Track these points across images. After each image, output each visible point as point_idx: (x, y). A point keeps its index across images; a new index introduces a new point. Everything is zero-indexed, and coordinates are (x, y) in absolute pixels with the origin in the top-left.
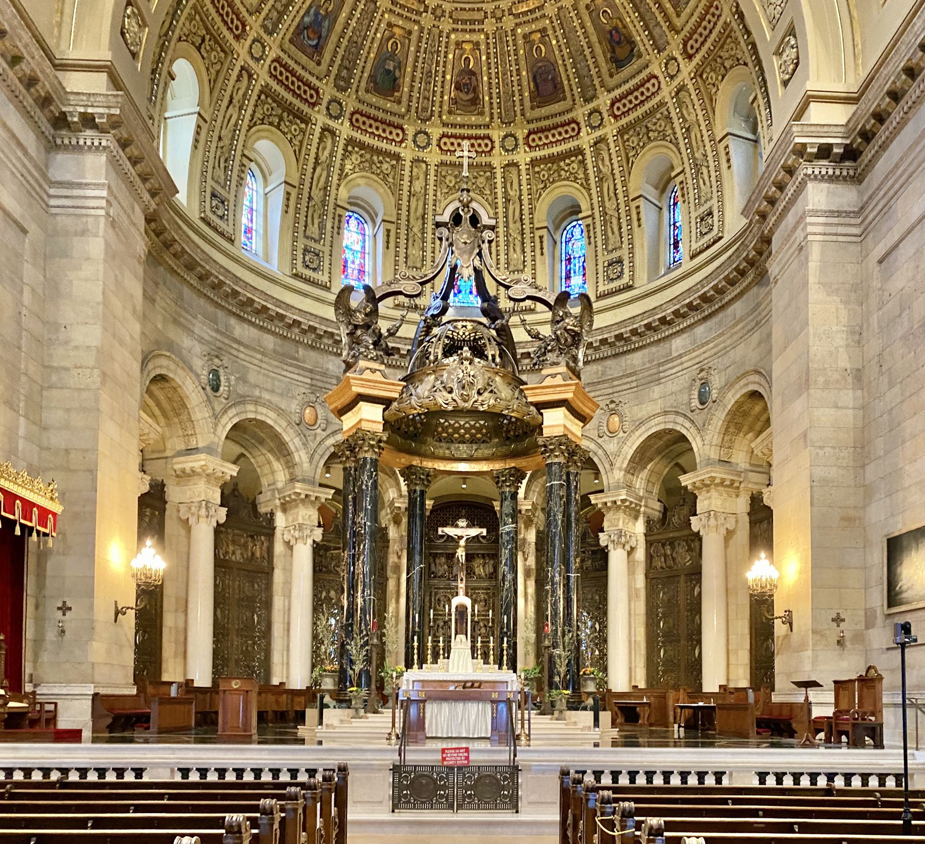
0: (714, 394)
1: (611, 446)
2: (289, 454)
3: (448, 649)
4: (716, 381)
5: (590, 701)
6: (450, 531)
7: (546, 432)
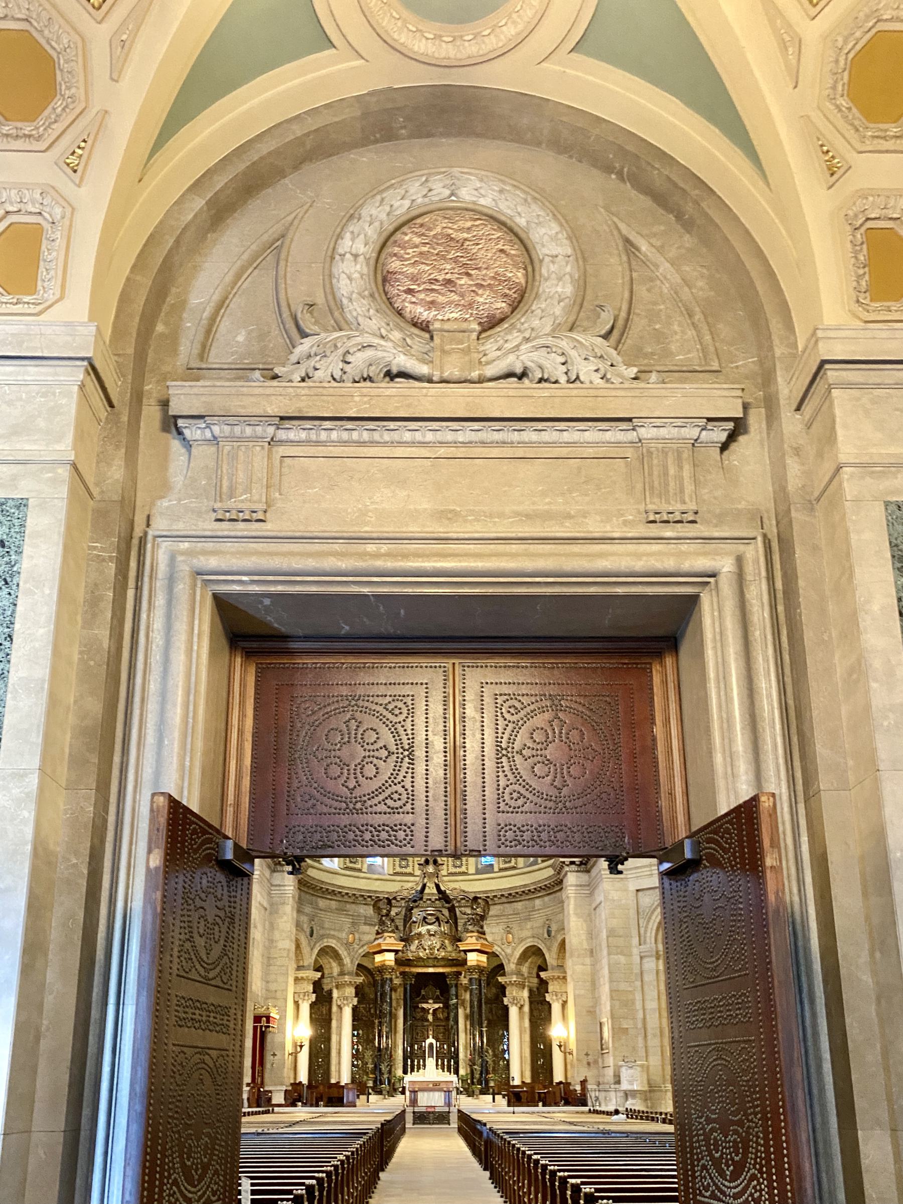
0: (553, 934)
1: (509, 951)
2: (342, 959)
3: (424, 1066)
4: (554, 928)
5: (491, 1090)
6: (425, 1006)
7: (469, 963)
